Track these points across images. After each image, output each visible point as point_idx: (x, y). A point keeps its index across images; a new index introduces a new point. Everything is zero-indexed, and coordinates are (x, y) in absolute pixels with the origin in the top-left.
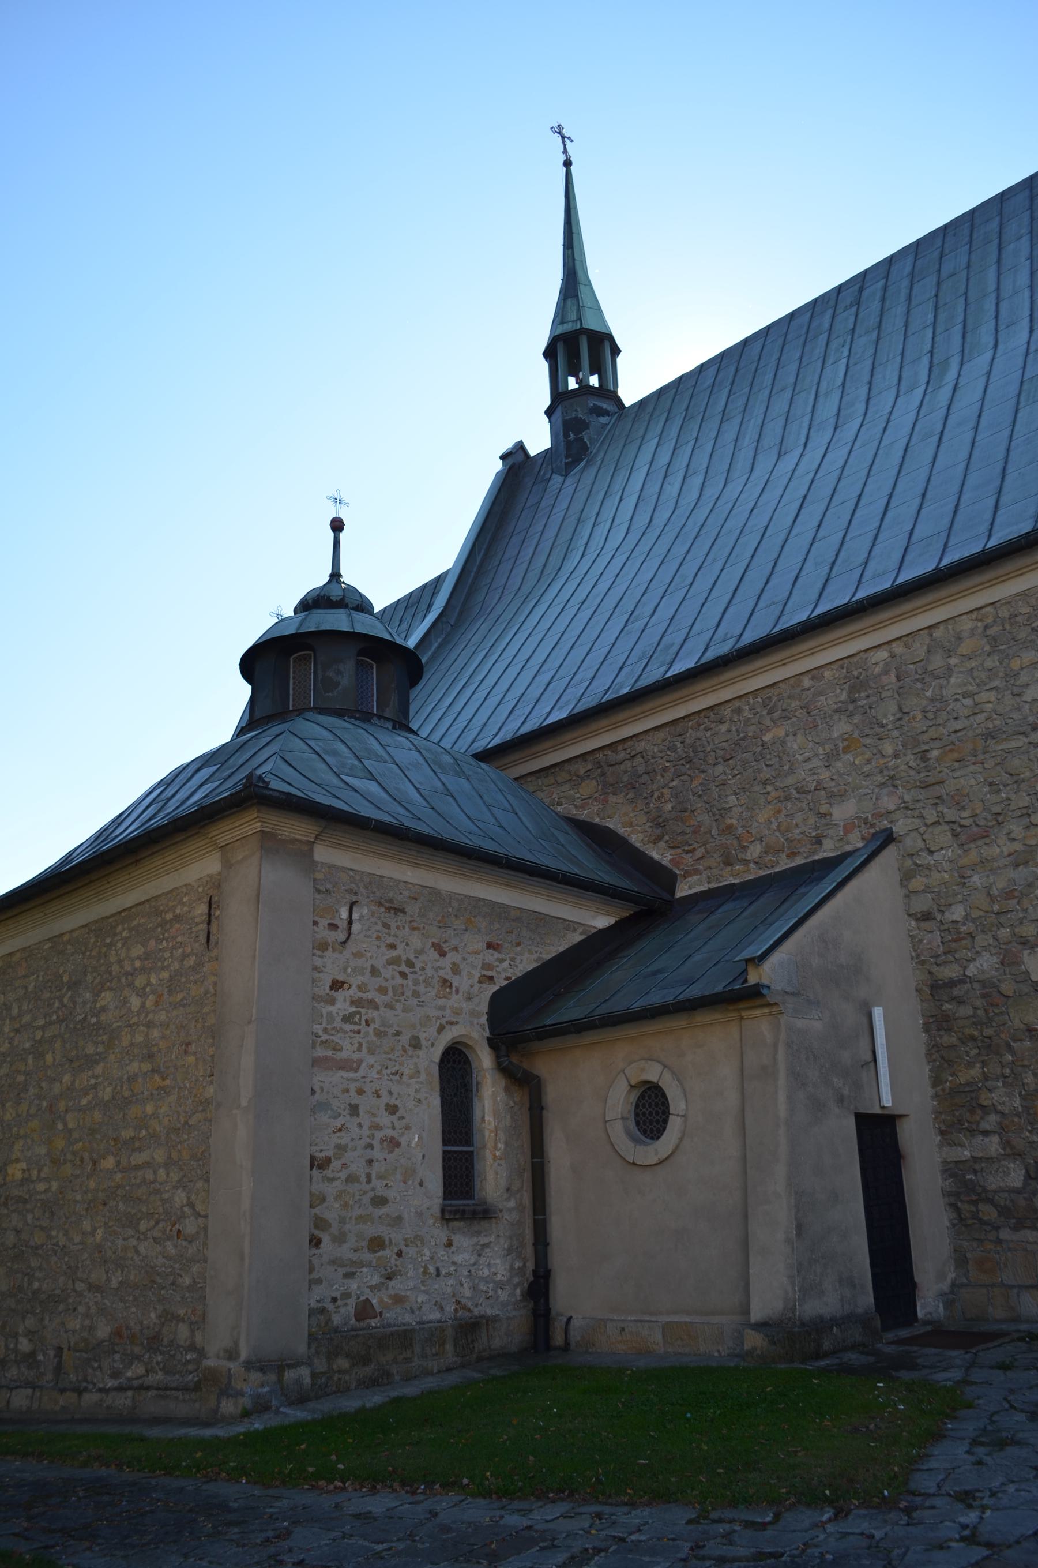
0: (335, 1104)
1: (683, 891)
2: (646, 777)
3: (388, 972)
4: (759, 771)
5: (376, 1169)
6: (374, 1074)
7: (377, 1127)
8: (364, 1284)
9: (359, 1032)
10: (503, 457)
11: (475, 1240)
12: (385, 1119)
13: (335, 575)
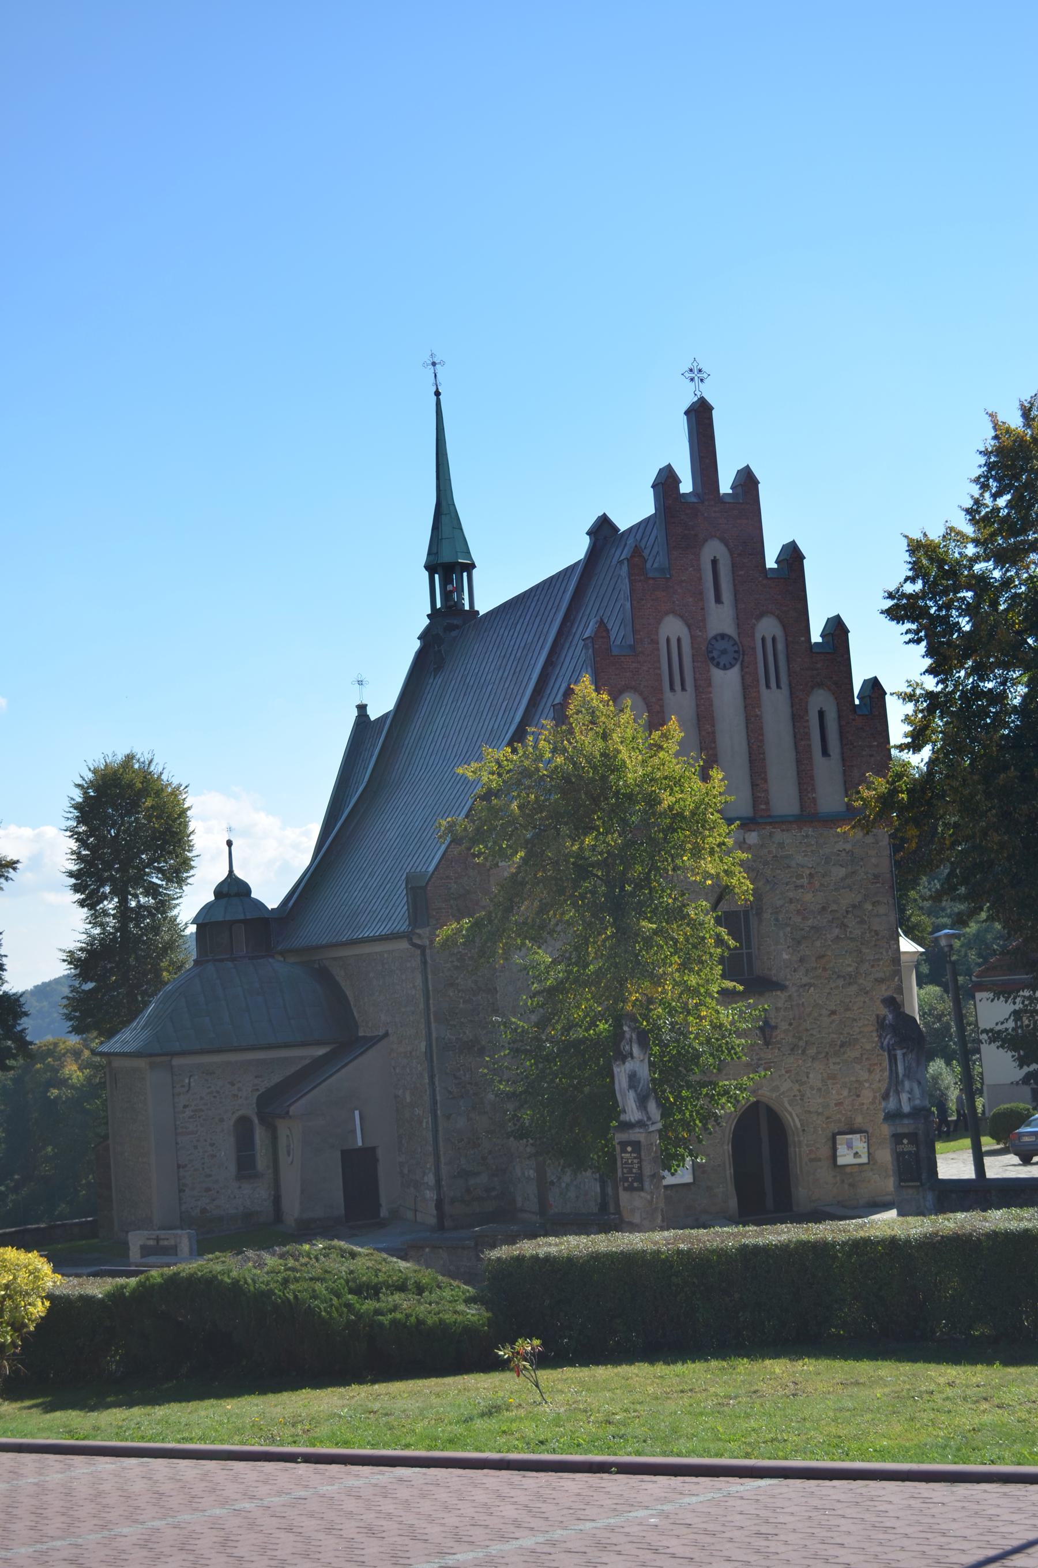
13: (231, 871)
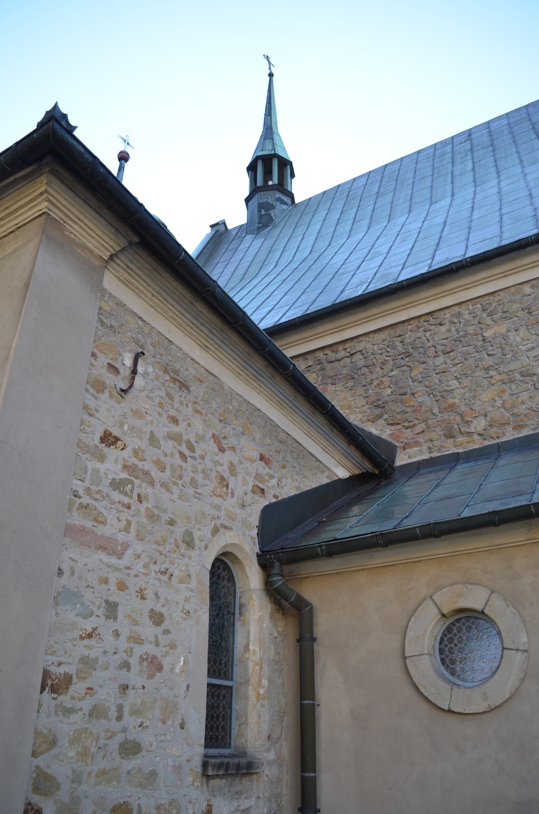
0: (88, 595)
1: (401, 460)
2: (365, 370)
3: (168, 446)
4: (481, 360)
5: (134, 698)
6: (139, 567)
7: (137, 640)
9: (129, 507)
10: (212, 226)
11: (235, 803)
12: (148, 630)
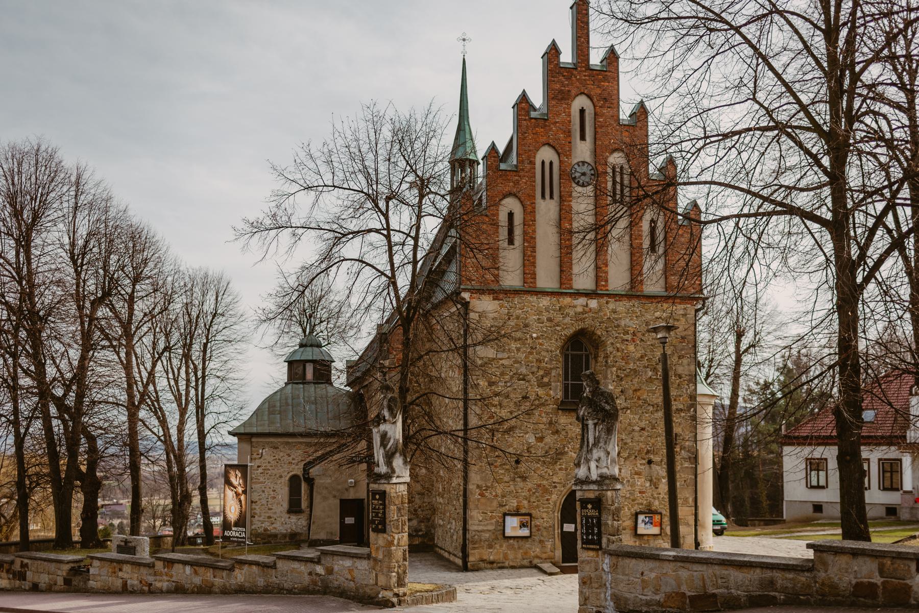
8: (266, 525)
